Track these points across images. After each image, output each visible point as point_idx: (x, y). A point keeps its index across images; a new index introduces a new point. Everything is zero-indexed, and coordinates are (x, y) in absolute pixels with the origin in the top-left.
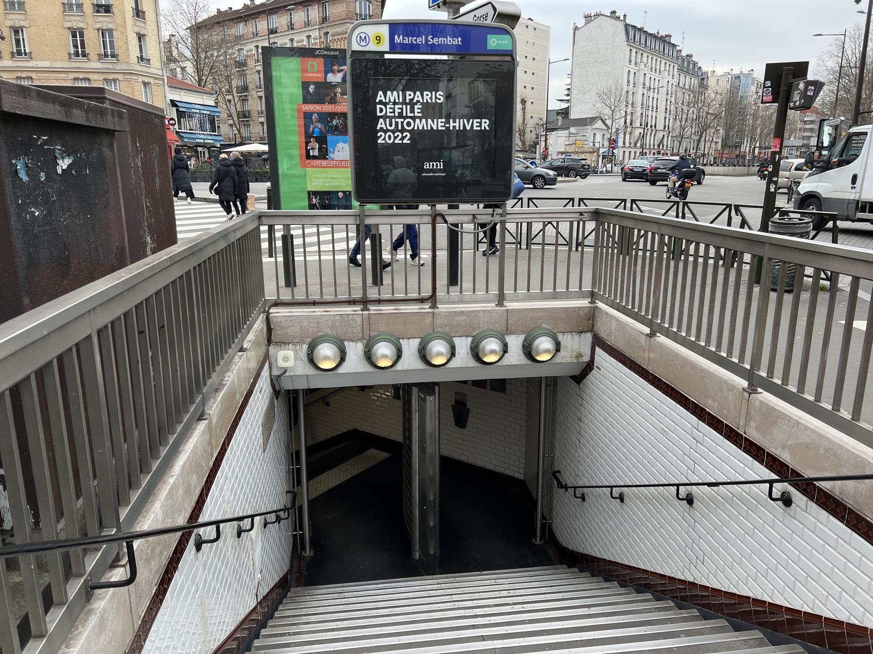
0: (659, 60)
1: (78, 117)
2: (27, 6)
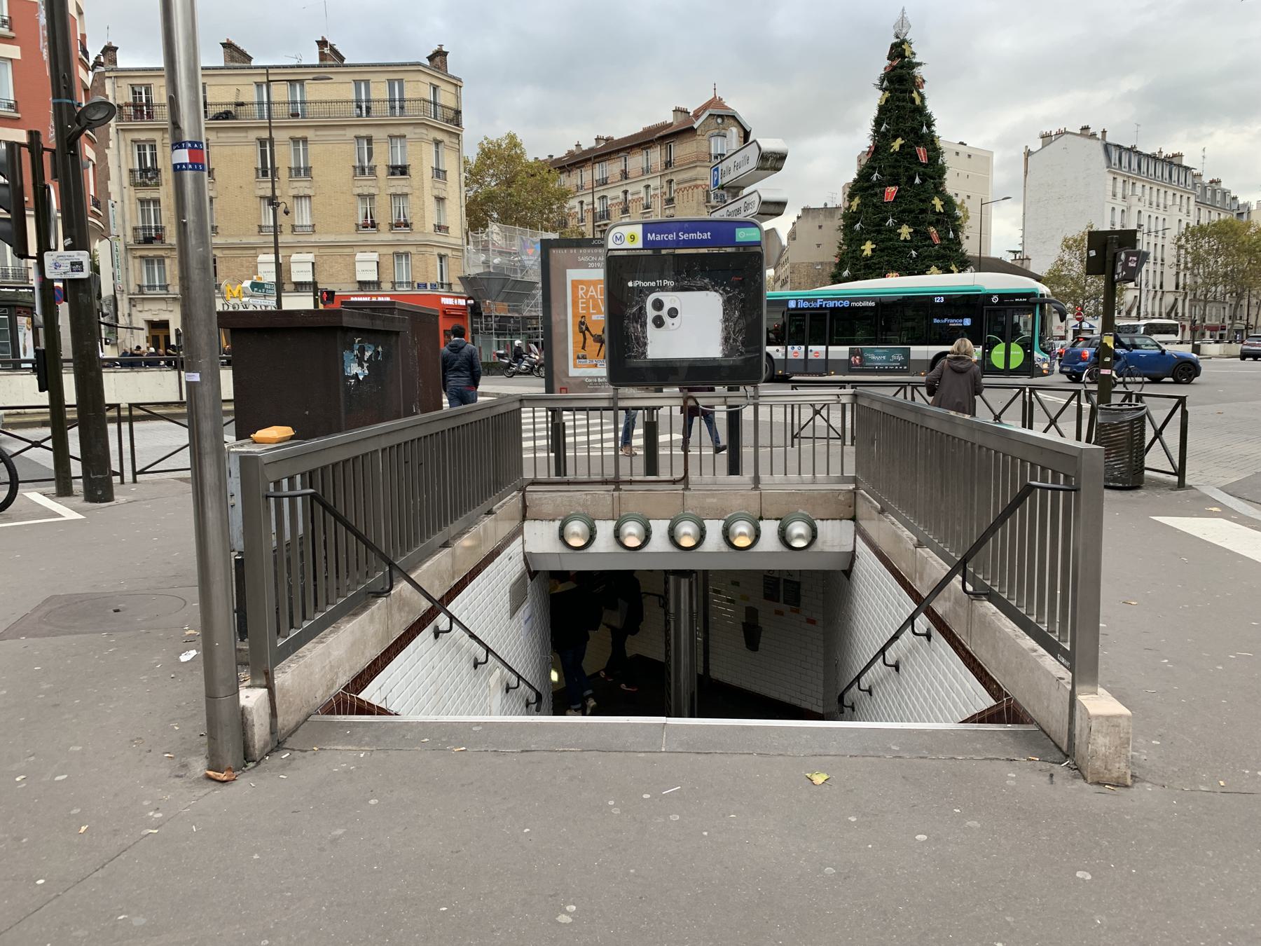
0: (1162, 191)
1: (379, 325)
2: (314, 172)
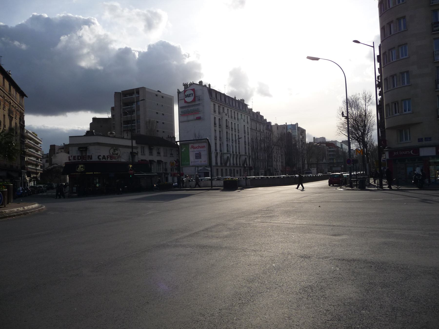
0: (236, 113)
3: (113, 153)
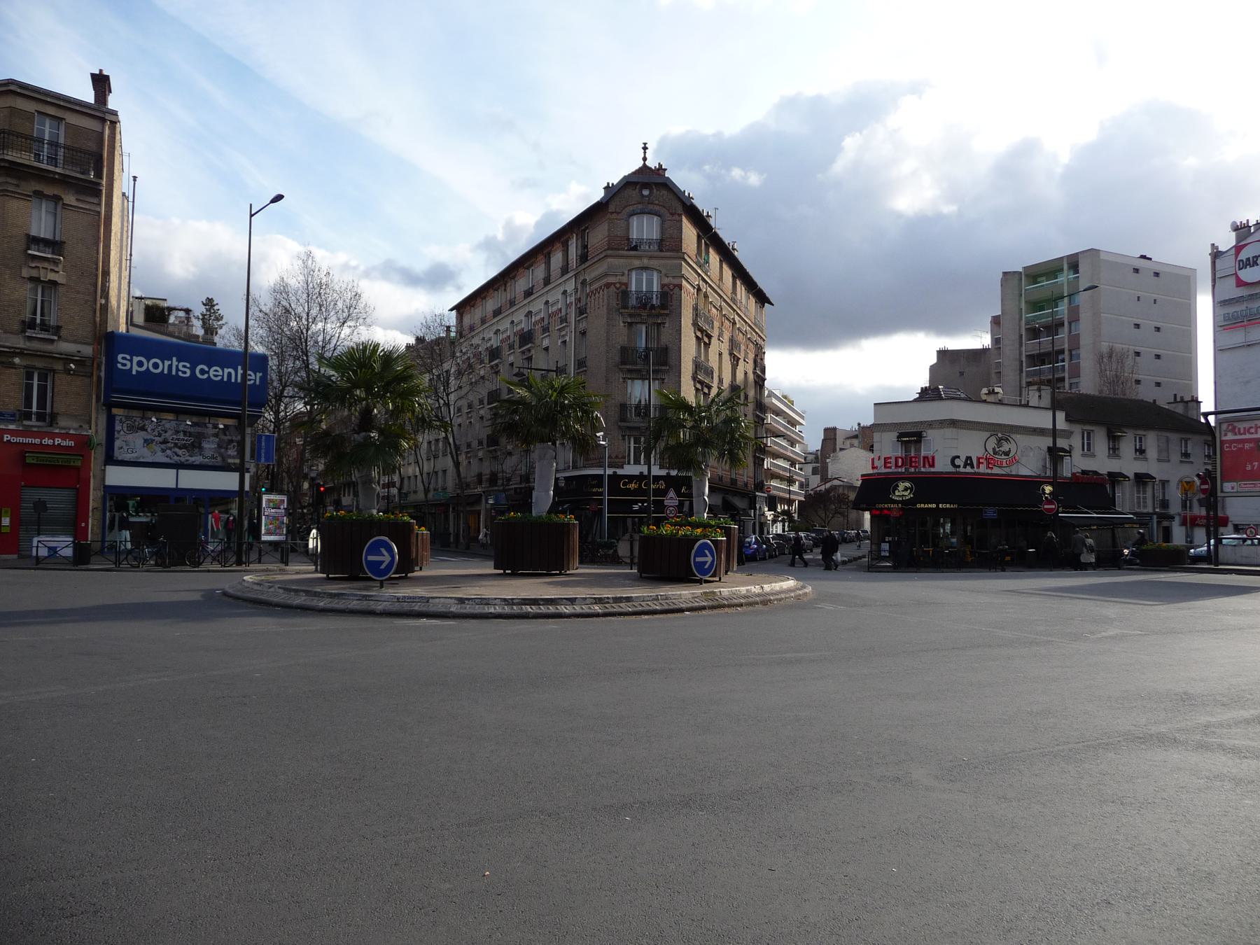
3: (994, 449)
